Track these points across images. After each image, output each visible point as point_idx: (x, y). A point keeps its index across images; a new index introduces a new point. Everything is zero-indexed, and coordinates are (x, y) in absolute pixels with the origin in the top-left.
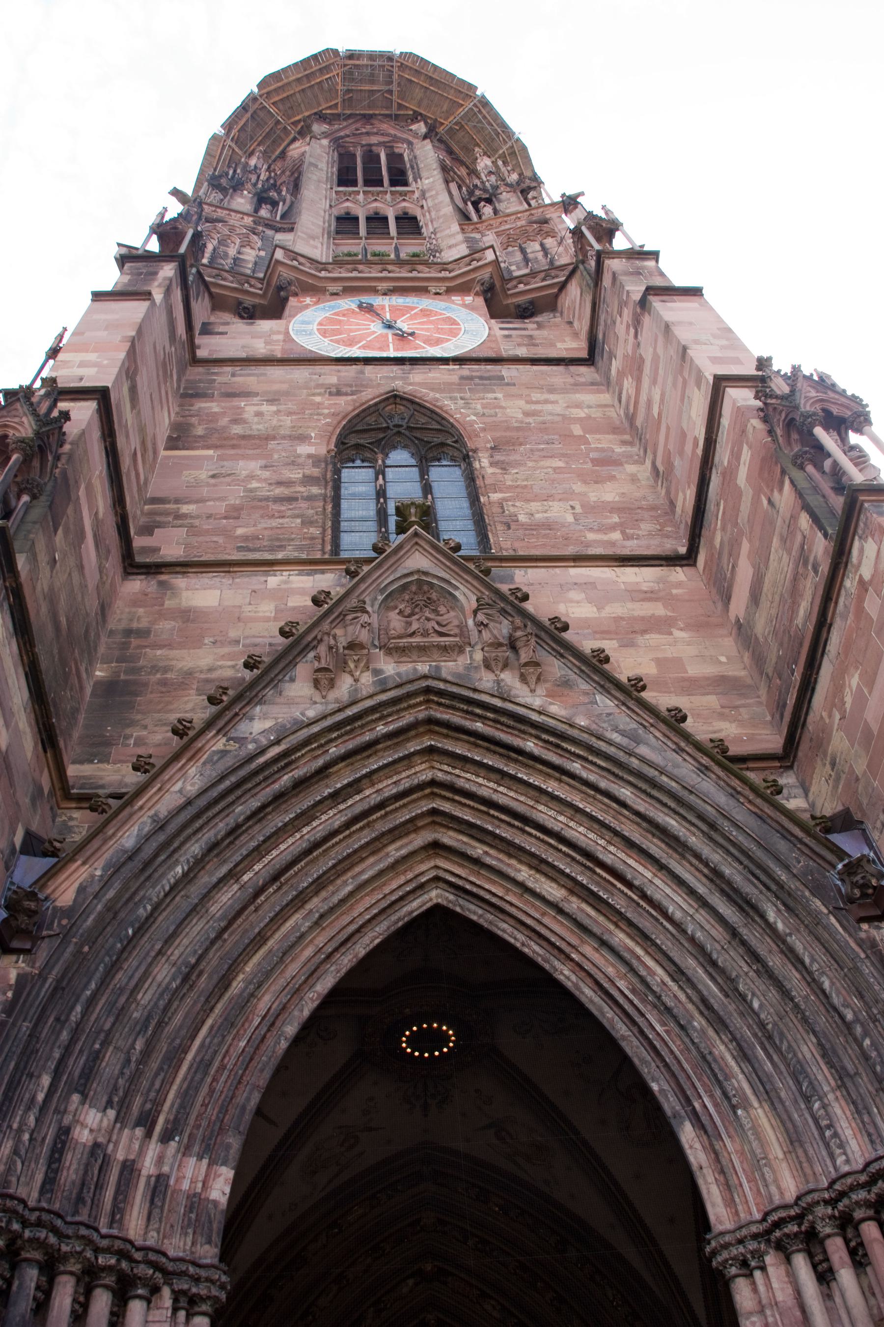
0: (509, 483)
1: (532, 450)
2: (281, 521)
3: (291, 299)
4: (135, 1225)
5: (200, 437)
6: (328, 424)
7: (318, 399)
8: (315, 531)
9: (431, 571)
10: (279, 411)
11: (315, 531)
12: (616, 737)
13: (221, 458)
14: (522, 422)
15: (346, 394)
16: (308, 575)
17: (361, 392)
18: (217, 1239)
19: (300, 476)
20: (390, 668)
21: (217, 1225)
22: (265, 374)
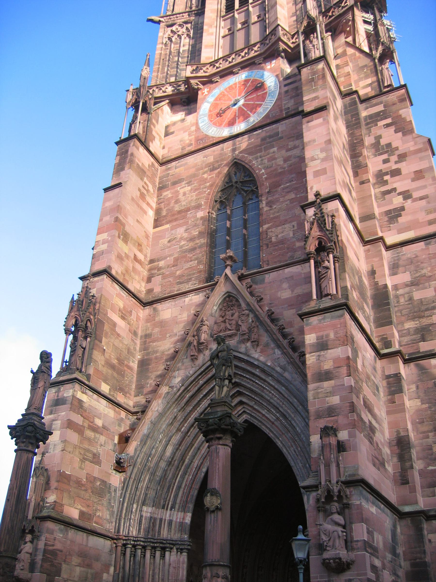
0: (272, 216)
1: (283, 189)
2: (190, 263)
3: (200, 92)
4: (165, 534)
5: (165, 216)
6: (209, 194)
7: (205, 176)
8: (201, 267)
9: (231, 291)
10: (191, 189)
11: (201, 267)
12: (278, 369)
13: (172, 229)
14: (282, 168)
15: (216, 169)
16: (198, 294)
18: (188, 532)
19: (197, 233)
21: (188, 528)
22: (186, 164)
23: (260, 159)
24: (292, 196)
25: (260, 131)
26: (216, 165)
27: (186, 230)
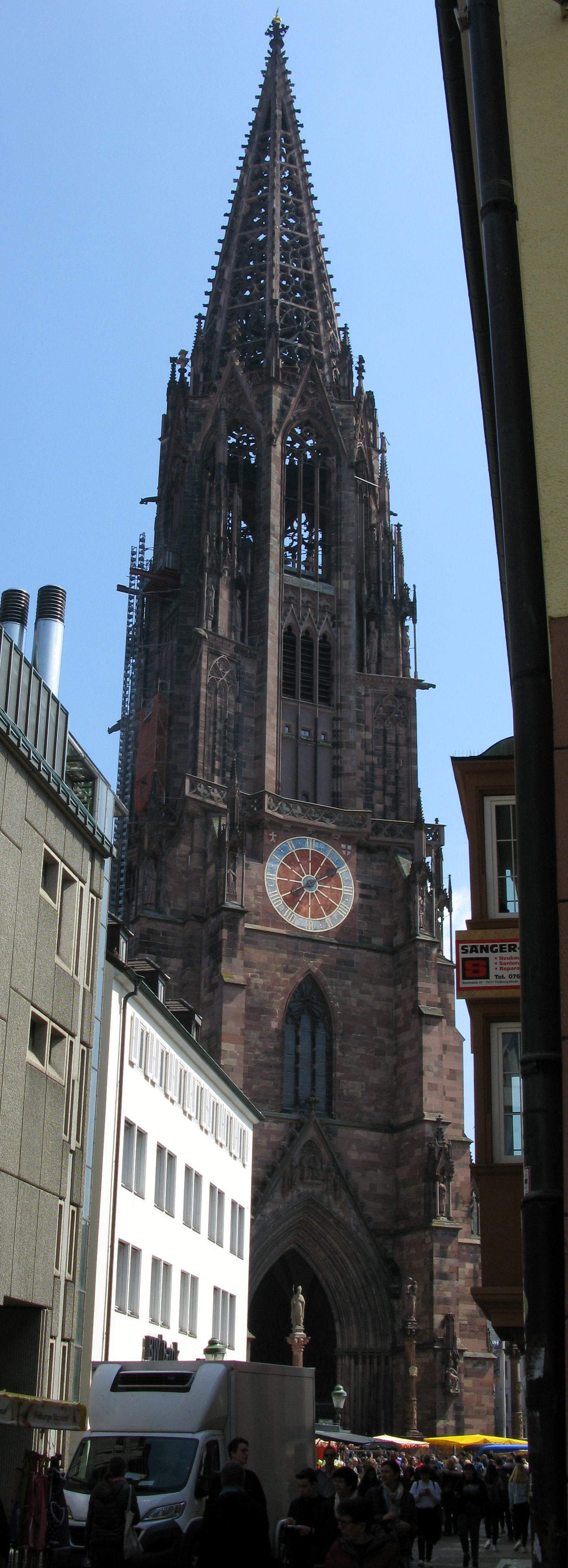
2: (267, 1082)
3: (266, 833)
8: (277, 1091)
10: (264, 985)
12: (353, 1228)
17: (296, 969)
19: (272, 1047)
20: (302, 1189)
23: (335, 987)
24: (362, 1051)
25: (336, 948)
26: (291, 966)
27: (260, 1038)
